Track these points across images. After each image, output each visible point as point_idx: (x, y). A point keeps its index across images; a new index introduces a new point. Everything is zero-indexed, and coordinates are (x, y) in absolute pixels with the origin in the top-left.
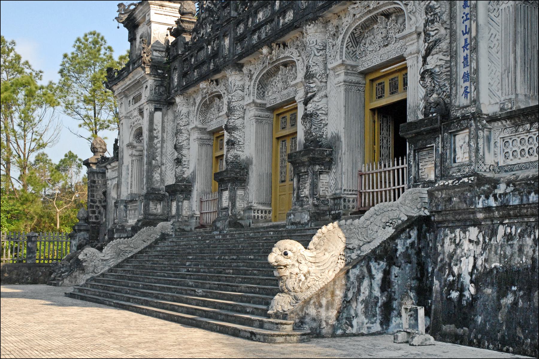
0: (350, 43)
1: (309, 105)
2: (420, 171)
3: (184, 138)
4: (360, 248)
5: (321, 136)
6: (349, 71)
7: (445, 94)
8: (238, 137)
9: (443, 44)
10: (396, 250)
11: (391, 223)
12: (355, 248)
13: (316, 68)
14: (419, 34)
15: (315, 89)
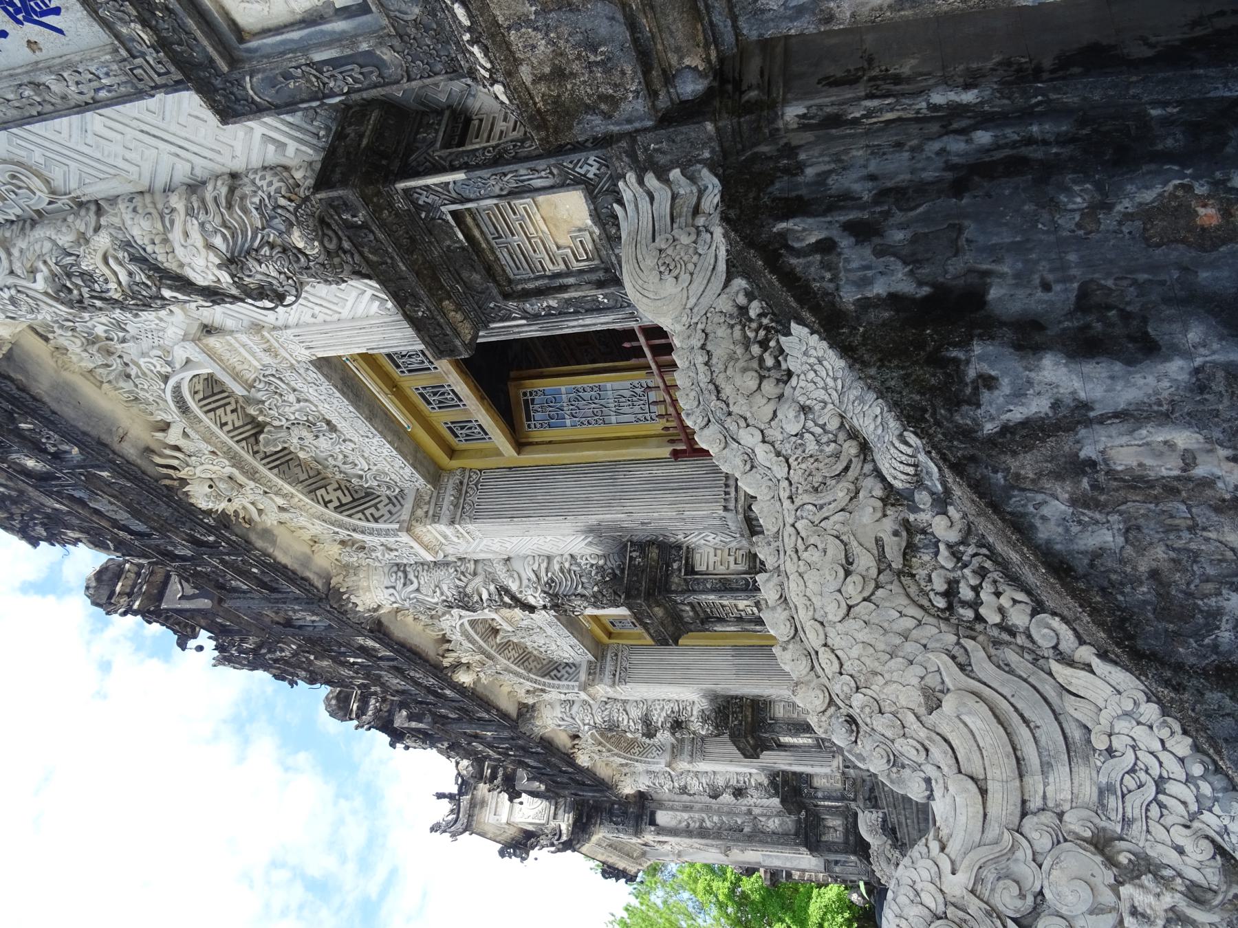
0: (367, 512)
1: (532, 601)
2: (576, 266)
3: (695, 782)
4: (892, 497)
5: (601, 569)
6: (431, 513)
7: (282, 202)
8: (664, 714)
9: (136, 232)
10: (894, 299)
11: (764, 344)
12: (906, 523)
13: (445, 588)
14: (208, 330)
15: (492, 587)
